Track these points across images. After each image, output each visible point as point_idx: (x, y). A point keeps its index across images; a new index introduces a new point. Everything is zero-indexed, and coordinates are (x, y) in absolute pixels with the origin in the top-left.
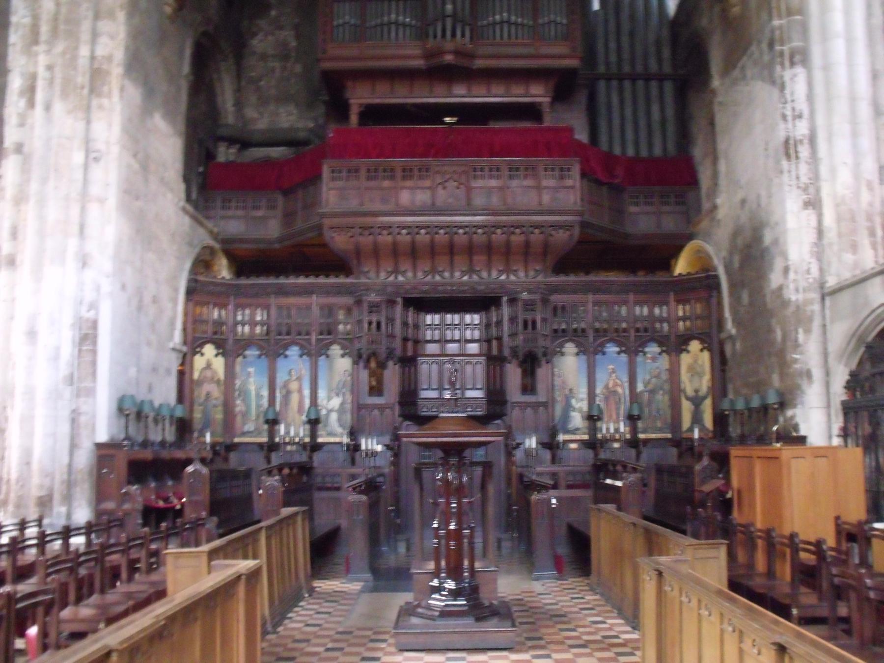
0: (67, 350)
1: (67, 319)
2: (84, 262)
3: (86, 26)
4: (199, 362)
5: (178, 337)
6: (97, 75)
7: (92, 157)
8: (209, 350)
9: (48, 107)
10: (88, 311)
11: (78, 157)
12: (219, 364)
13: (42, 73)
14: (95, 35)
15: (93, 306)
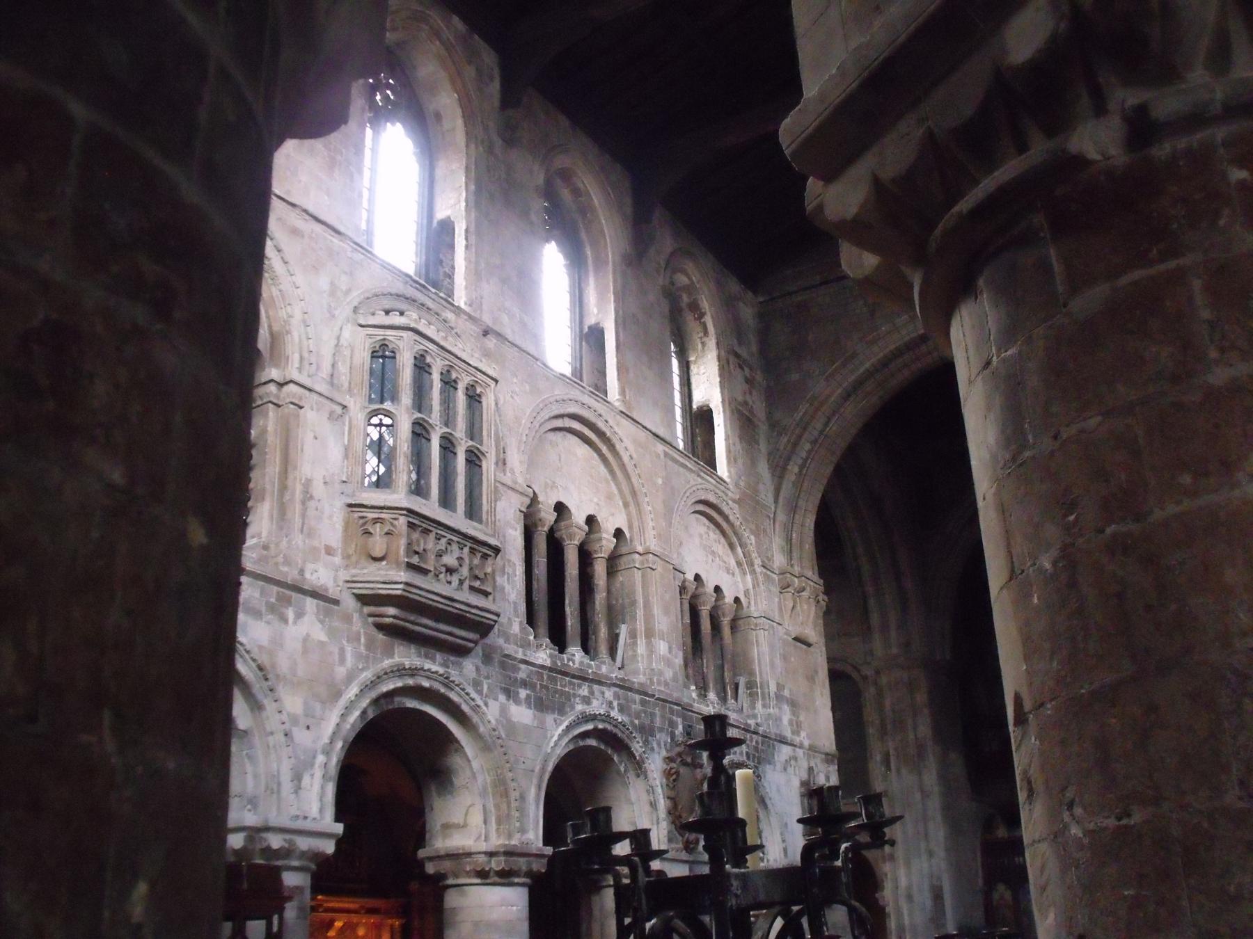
0: (929, 903)
1: (926, 886)
2: (931, 854)
3: (910, 722)
4: (996, 896)
5: (980, 882)
6: (921, 748)
7: (925, 794)
8: (1001, 888)
9: (898, 771)
10: (937, 882)
11: (918, 796)
12: (1008, 895)
13: (892, 752)
14: (915, 728)
15: (939, 879)
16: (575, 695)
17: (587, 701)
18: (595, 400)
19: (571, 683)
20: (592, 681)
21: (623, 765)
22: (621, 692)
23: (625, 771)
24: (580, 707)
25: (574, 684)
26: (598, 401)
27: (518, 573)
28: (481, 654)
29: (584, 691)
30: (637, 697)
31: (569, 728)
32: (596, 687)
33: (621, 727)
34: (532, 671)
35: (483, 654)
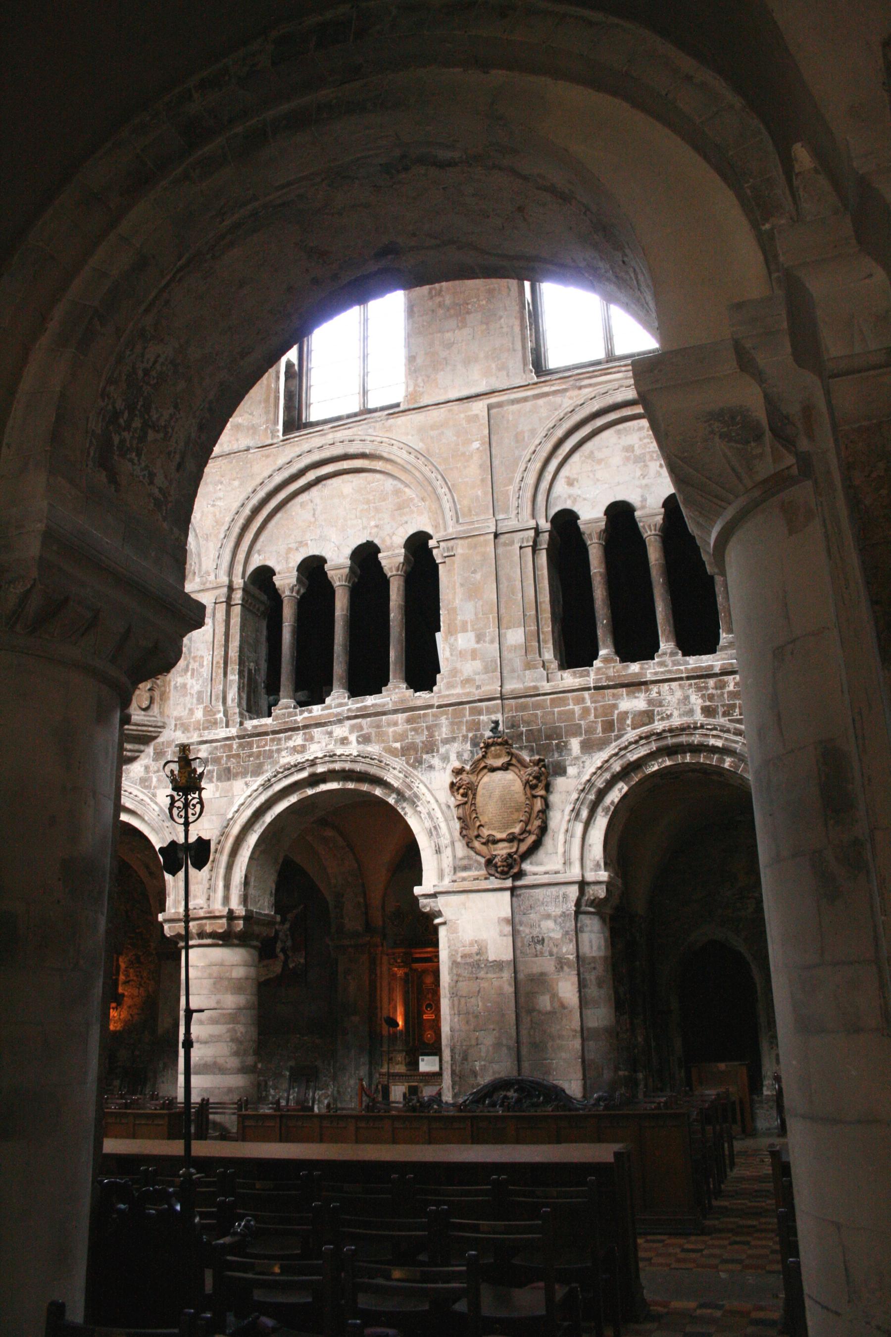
16: (279, 751)
17: (303, 749)
18: (346, 429)
19: (272, 740)
20: (306, 727)
21: (394, 796)
22: (364, 722)
23: (396, 802)
24: (286, 759)
25: (280, 739)
26: (349, 428)
27: (205, 663)
28: (152, 754)
29: (298, 739)
30: (401, 717)
31: (267, 785)
32: (317, 732)
33: (363, 760)
34: (216, 748)
35: (154, 753)
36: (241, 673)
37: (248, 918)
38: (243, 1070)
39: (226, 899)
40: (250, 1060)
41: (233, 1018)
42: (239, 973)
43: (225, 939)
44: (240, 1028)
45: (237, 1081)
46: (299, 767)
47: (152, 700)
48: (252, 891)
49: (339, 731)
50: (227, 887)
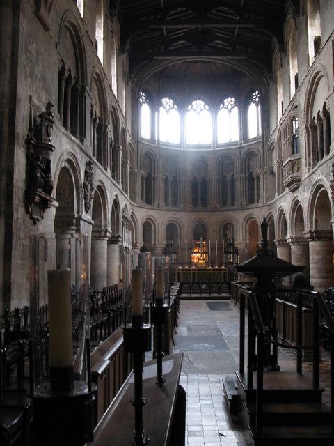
31: (312, 191)
36: (313, 155)
37: (316, 232)
38: (321, 277)
39: (311, 227)
40: (324, 275)
41: (317, 262)
42: (318, 249)
43: (313, 238)
44: (319, 266)
45: (319, 281)
46: (314, 185)
47: (298, 168)
48: (319, 223)
49: (319, 171)
50: (311, 223)
